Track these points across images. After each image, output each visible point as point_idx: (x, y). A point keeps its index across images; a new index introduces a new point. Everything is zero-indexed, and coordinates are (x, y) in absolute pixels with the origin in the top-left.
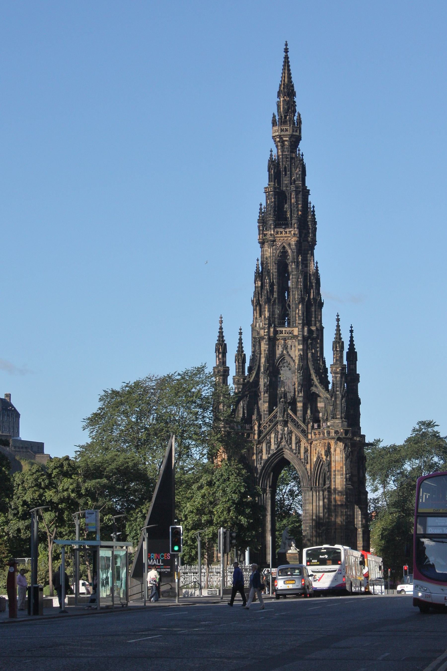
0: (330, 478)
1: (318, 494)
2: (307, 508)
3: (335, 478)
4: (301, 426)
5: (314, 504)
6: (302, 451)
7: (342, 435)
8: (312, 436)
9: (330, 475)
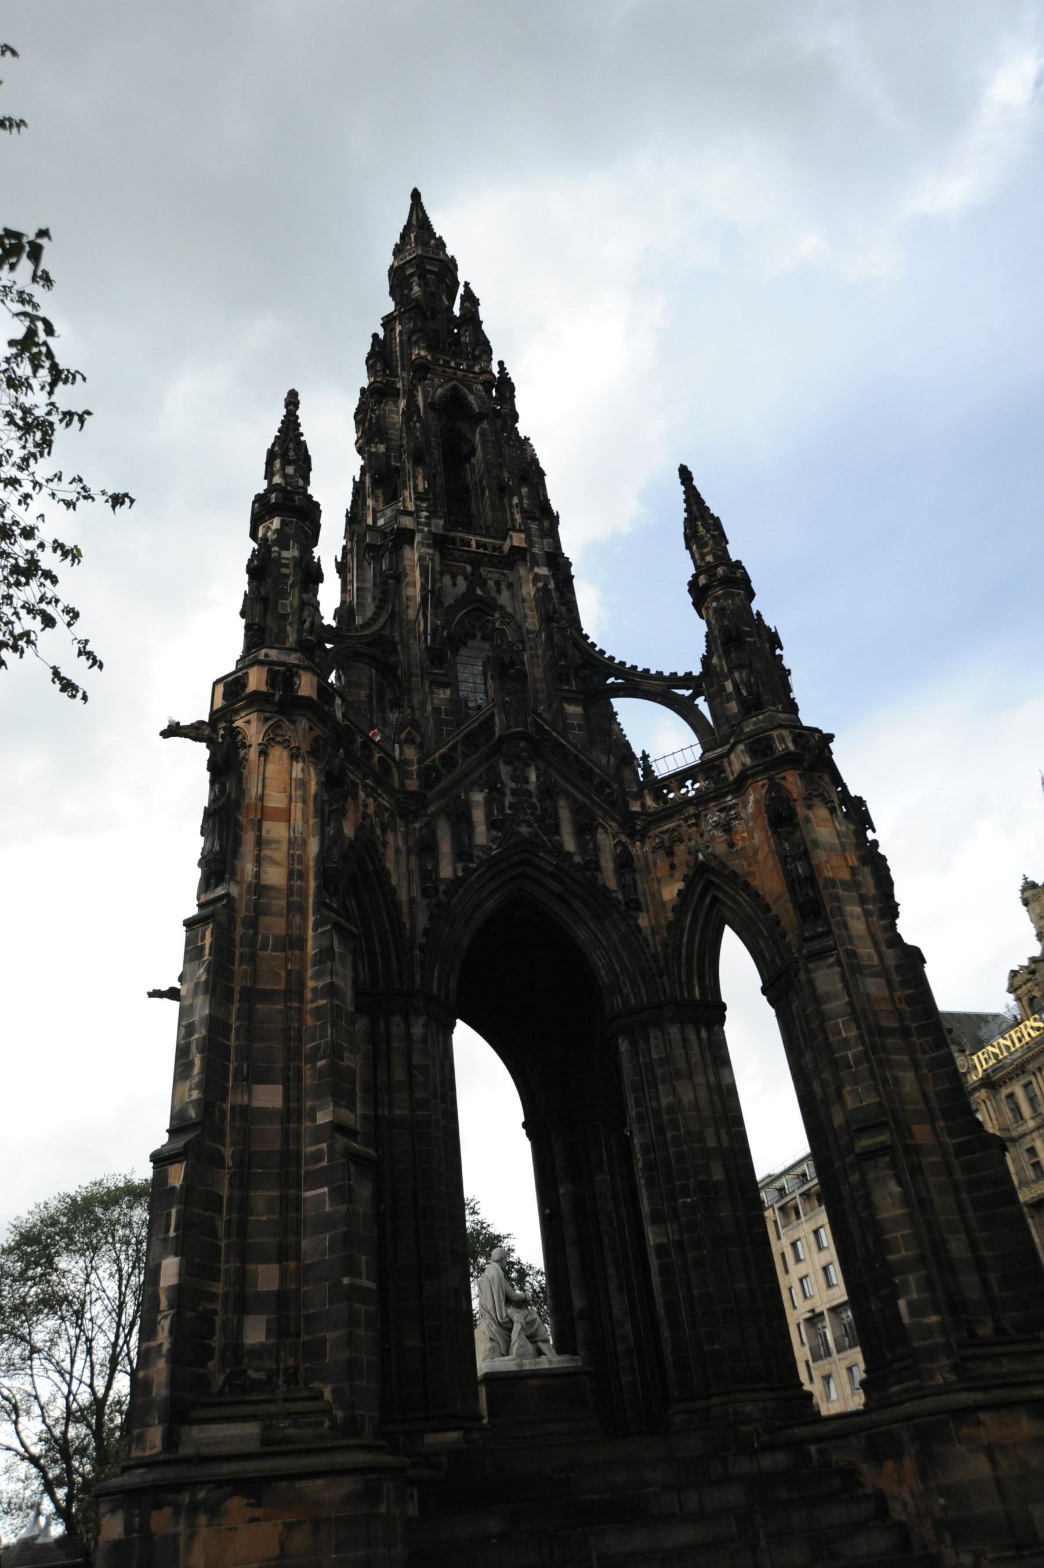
1: (704, 1034)
2: (665, 1100)
3: (841, 911)
4: (591, 771)
5: (700, 1079)
6: (607, 863)
8: (643, 805)
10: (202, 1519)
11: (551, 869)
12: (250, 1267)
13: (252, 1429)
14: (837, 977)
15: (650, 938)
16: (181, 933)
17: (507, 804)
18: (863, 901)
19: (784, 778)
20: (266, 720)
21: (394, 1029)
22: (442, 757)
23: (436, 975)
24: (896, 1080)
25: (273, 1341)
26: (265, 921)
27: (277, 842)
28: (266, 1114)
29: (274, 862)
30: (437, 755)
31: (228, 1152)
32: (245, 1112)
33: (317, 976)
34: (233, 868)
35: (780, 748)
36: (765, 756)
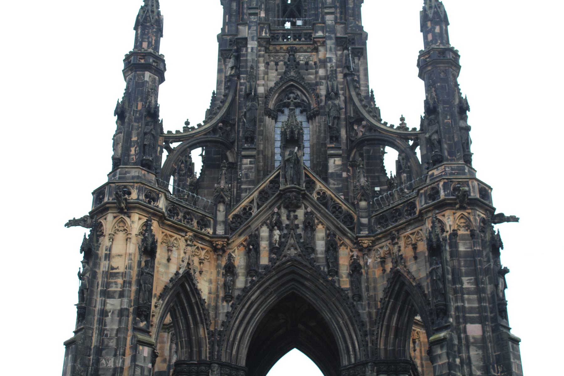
16: (63, 348)
19: (444, 216)
20: (115, 217)
36: (434, 200)
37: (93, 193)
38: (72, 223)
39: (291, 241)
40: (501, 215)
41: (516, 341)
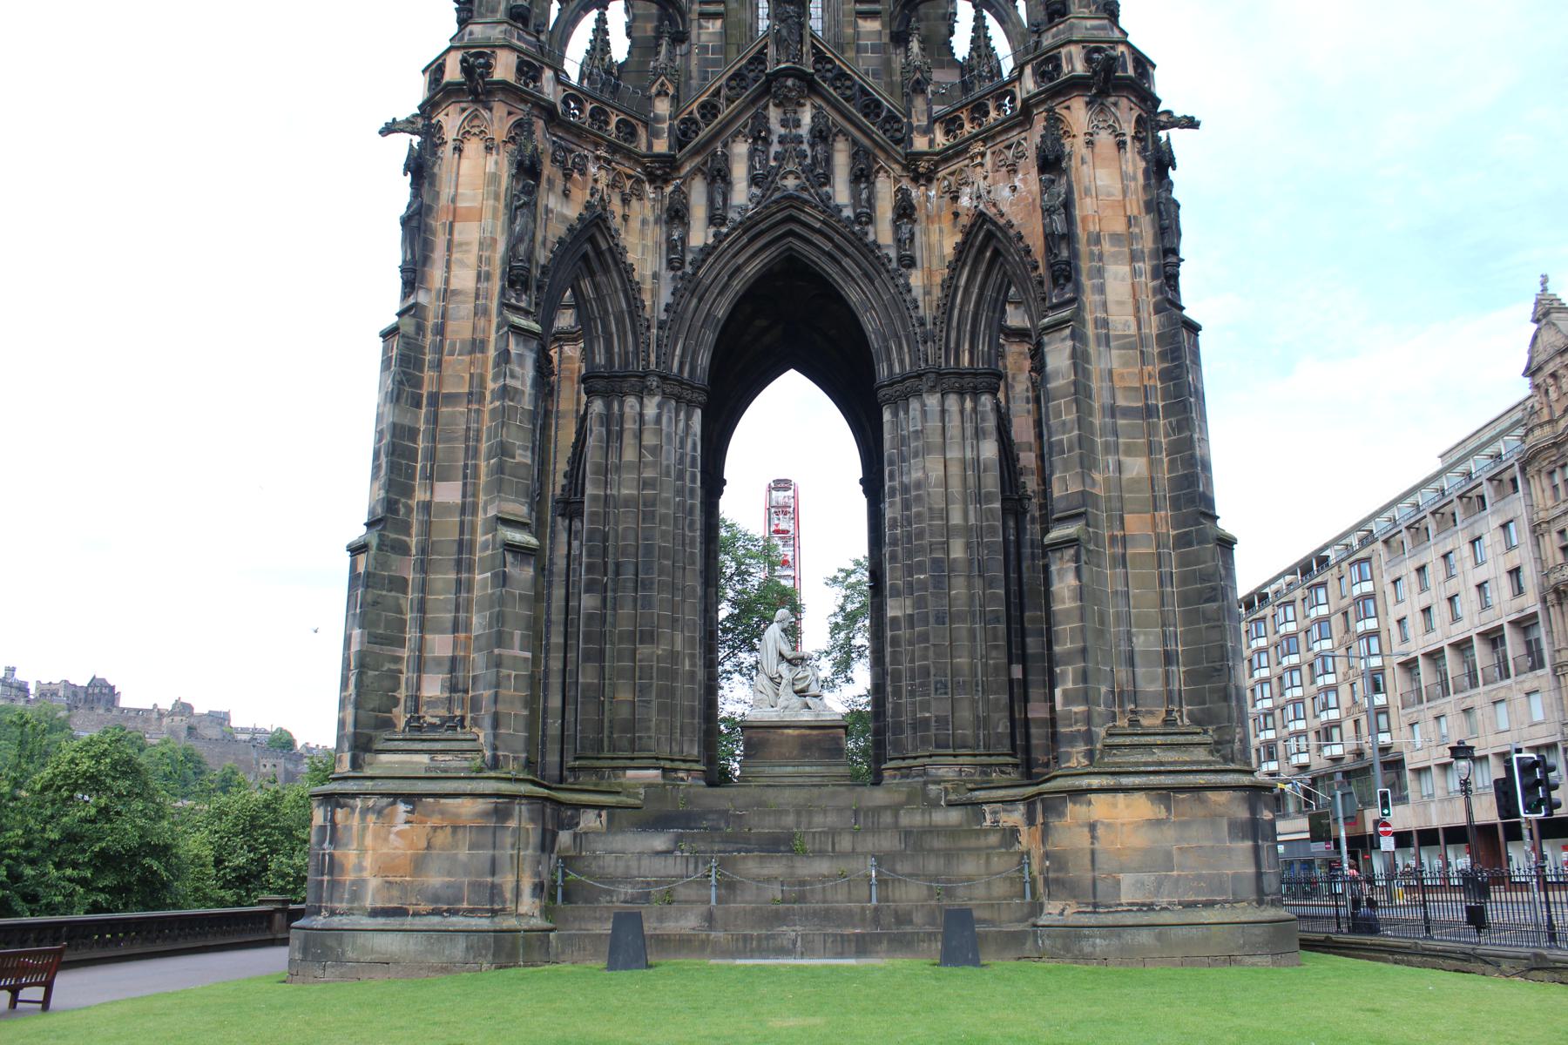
0: (1065, 274)
1: (968, 404)
2: (917, 475)
3: (1100, 272)
4: (878, 104)
5: (954, 453)
7: (1125, 70)
8: (931, 142)
9: (1075, 254)
10: (372, 818)
11: (818, 225)
12: (428, 636)
13: (425, 758)
14: (1067, 352)
15: (920, 299)
16: (379, 343)
17: (772, 155)
18: (1134, 257)
20: (464, 110)
21: (627, 409)
22: (703, 106)
23: (678, 352)
24: (1119, 465)
25: (447, 695)
26: (451, 326)
27: (467, 244)
28: (446, 508)
29: (462, 264)
30: (695, 106)
31: (413, 542)
32: (427, 507)
33: (495, 379)
34: (423, 275)
35: (1066, 68)
36: (1051, 80)
37: (424, 72)
38: (389, 129)
39: (791, 167)
40: (1169, 113)
41: (1194, 328)
